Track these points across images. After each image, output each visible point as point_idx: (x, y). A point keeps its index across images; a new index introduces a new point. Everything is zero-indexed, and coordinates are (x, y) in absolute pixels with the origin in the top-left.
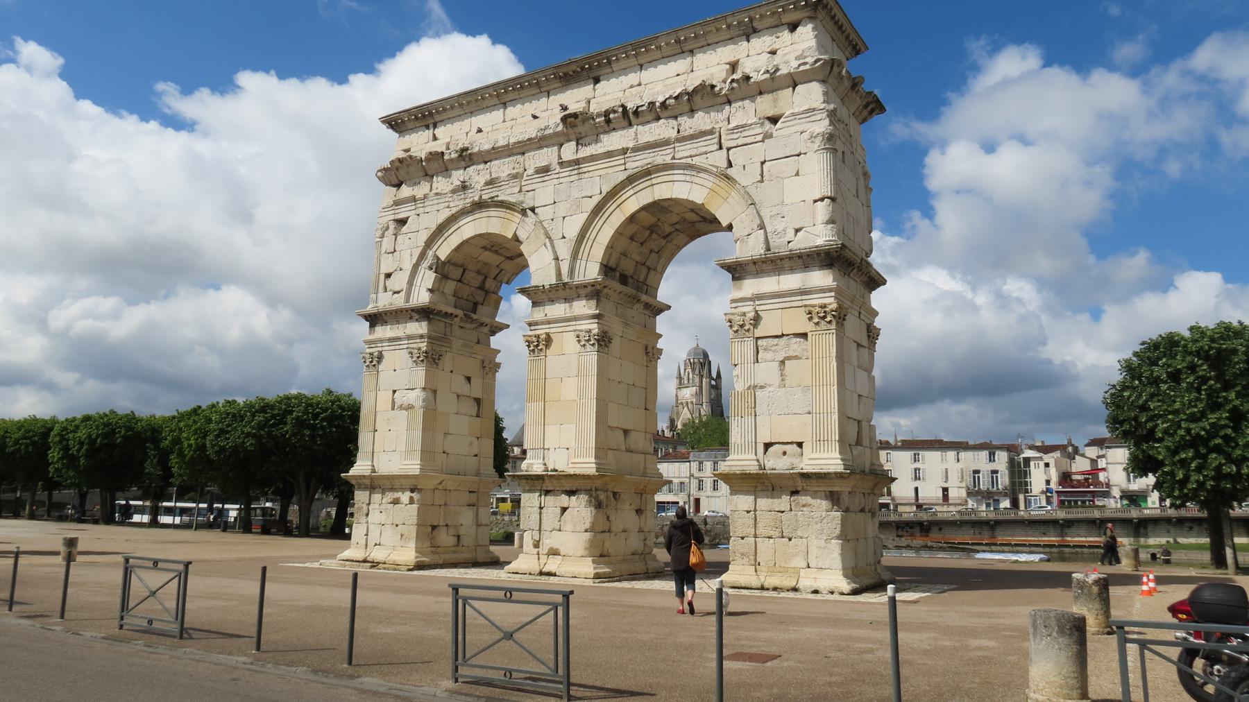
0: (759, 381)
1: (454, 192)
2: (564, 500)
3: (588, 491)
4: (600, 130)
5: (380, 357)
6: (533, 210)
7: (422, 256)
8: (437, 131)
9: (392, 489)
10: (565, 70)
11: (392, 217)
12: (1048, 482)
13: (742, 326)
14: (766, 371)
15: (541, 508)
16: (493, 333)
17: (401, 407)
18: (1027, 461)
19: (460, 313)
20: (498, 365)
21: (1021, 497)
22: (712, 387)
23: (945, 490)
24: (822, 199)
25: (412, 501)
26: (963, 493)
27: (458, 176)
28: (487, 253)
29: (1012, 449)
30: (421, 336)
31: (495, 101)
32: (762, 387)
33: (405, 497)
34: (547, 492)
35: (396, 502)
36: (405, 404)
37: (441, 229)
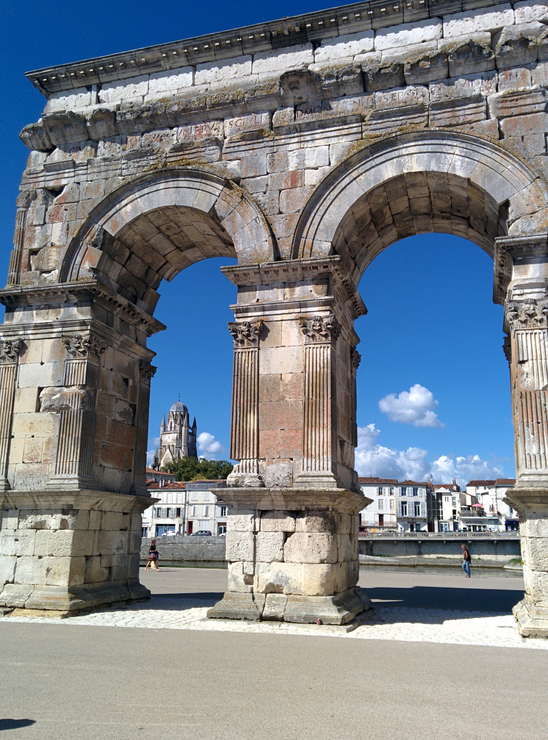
1: (128, 158)
2: (288, 523)
3: (323, 512)
4: (329, 95)
5: (22, 348)
7: (85, 229)
8: (102, 93)
9: (36, 511)
10: (279, 29)
11: (42, 185)
12: (454, 512)
13: (531, 316)
15: (255, 533)
16: (149, 333)
17: (49, 409)
18: (440, 495)
19: (123, 301)
20: (154, 369)
21: (436, 523)
22: (189, 434)
23: (381, 516)
25: (64, 525)
26: (394, 519)
27: (136, 142)
28: (160, 236)
29: (429, 487)
30: (83, 323)
31: (183, 61)
33: (54, 521)
34: (263, 514)
35: (39, 526)
37: (112, 200)
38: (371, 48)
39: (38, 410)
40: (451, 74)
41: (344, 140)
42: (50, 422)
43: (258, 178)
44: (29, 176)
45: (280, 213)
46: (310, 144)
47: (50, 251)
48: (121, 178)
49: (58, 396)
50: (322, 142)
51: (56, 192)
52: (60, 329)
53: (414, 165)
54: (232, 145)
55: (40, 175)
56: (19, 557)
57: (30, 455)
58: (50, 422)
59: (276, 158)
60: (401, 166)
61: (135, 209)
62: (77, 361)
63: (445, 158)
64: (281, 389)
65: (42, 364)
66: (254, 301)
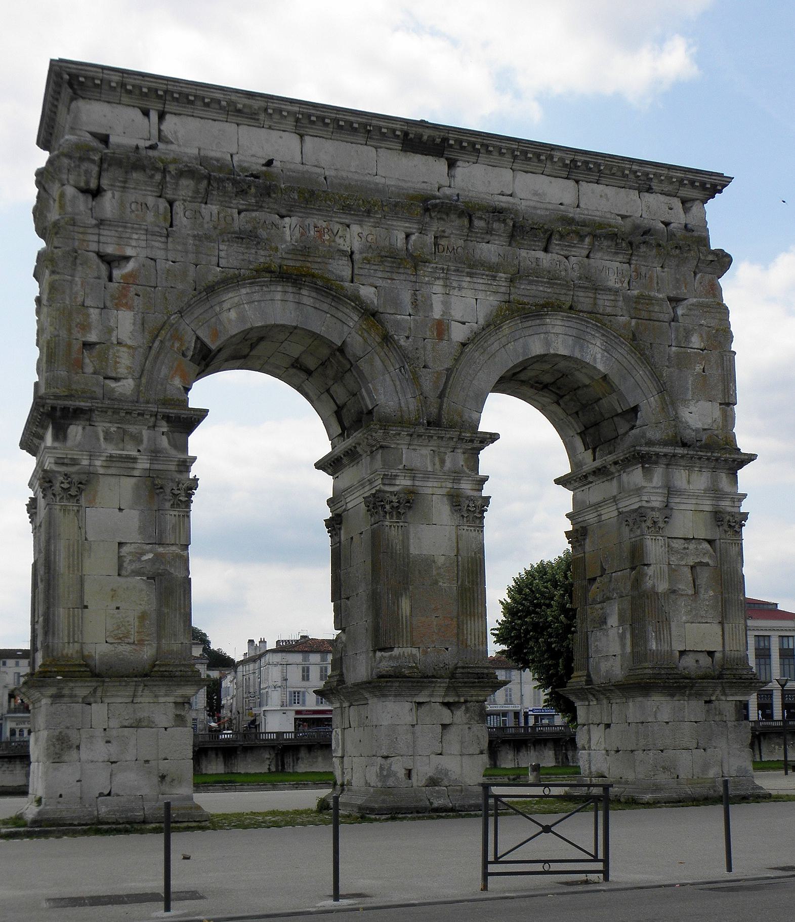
17: (137, 573)
38: (510, 193)
40: (591, 255)
41: (491, 298)
42: (142, 590)
43: (399, 317)
44: (71, 228)
45: (424, 367)
46: (456, 292)
47: (118, 351)
48: (219, 269)
49: (150, 556)
50: (469, 293)
51: (110, 261)
52: (147, 466)
53: (561, 347)
54: (368, 266)
55: (90, 231)
57: (116, 632)
58: (142, 590)
59: (419, 297)
60: (548, 344)
61: (242, 318)
62: (177, 513)
63: (588, 347)
64: (434, 573)
65: (120, 510)
66: (401, 467)
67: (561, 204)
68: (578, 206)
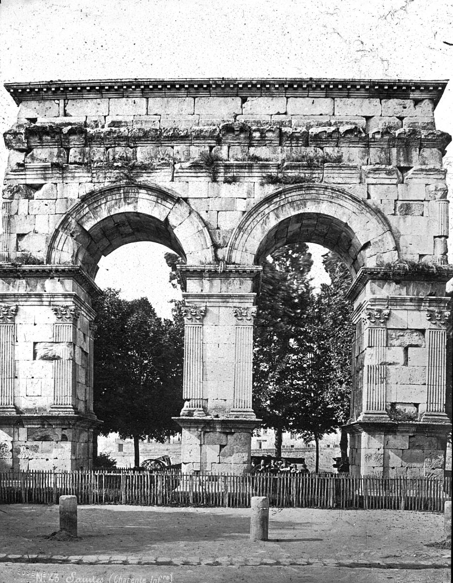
0: (389, 360)
6: (186, 200)
14: (396, 354)
17: (45, 358)
24: (440, 237)
32: (390, 364)
36: (50, 355)
38: (283, 112)
39: (34, 358)
56: (29, 459)
65: (35, 324)
67: (321, 115)
68: (334, 115)
